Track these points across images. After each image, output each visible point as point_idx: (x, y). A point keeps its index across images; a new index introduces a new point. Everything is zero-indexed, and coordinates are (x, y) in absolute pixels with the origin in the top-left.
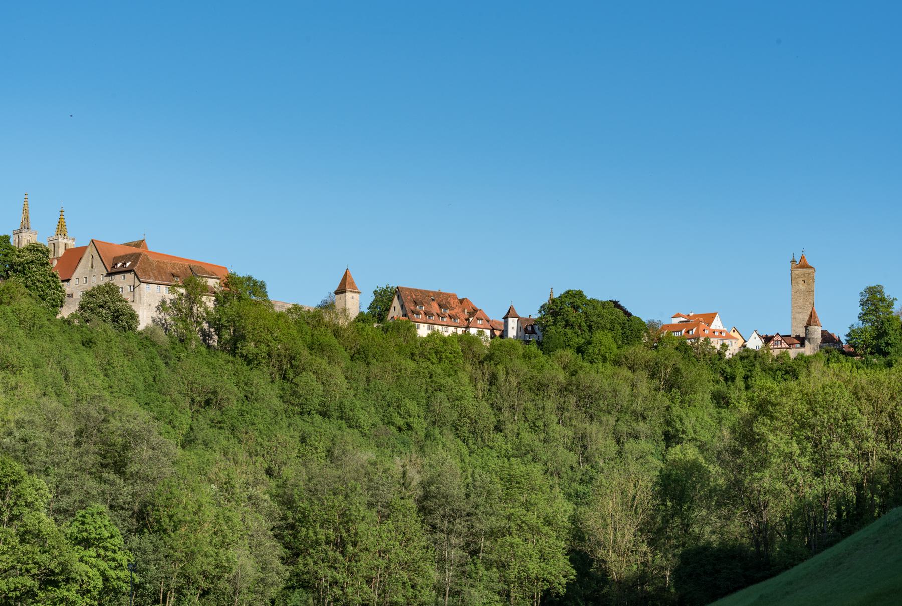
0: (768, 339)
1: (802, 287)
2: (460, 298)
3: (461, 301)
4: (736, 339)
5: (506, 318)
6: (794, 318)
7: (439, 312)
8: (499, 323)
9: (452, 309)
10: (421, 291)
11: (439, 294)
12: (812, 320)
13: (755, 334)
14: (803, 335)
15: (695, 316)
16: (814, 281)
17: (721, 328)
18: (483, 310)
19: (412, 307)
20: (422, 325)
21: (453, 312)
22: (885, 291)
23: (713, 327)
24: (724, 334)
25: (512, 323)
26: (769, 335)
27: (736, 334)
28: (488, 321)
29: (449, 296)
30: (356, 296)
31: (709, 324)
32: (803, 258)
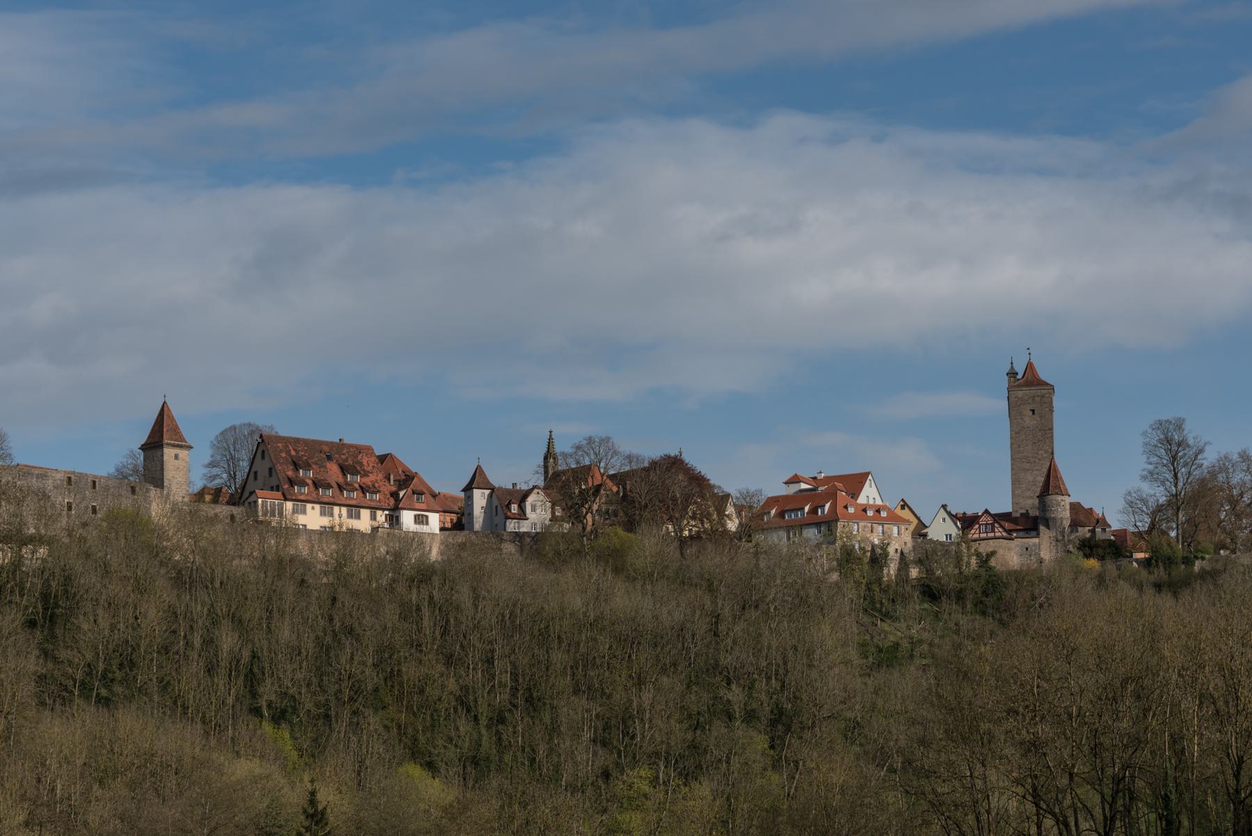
0: (967, 522)
1: (1029, 421)
2: (378, 453)
3: (382, 459)
4: (908, 522)
5: (468, 489)
6: (1016, 482)
7: (341, 480)
8: (454, 499)
9: (366, 474)
10: (306, 442)
11: (341, 446)
12: (1051, 484)
13: (943, 514)
14: (1034, 513)
15: (828, 479)
16: (1051, 411)
17: (879, 502)
18: (422, 474)
19: (290, 473)
20: (309, 506)
21: (367, 481)
22: (1187, 427)
23: (862, 500)
24: (884, 514)
25: (480, 498)
26: (969, 512)
27: (906, 514)
28: (434, 496)
29: (359, 449)
30: (183, 453)
31: (855, 494)
32: (1030, 366)
